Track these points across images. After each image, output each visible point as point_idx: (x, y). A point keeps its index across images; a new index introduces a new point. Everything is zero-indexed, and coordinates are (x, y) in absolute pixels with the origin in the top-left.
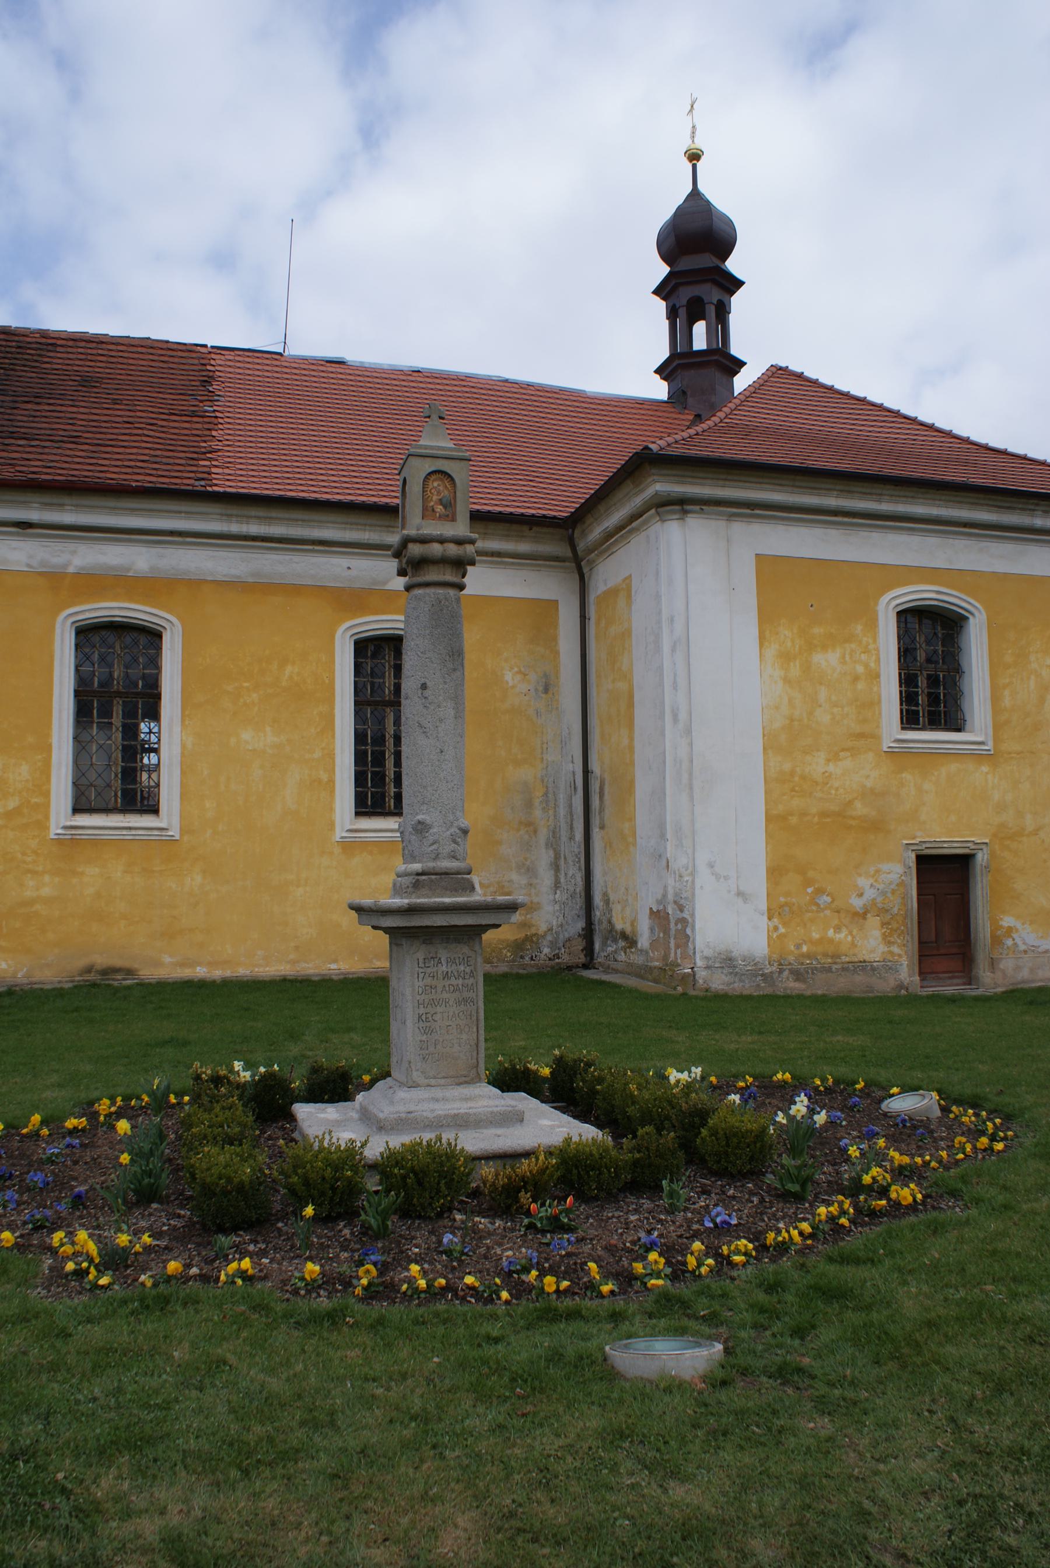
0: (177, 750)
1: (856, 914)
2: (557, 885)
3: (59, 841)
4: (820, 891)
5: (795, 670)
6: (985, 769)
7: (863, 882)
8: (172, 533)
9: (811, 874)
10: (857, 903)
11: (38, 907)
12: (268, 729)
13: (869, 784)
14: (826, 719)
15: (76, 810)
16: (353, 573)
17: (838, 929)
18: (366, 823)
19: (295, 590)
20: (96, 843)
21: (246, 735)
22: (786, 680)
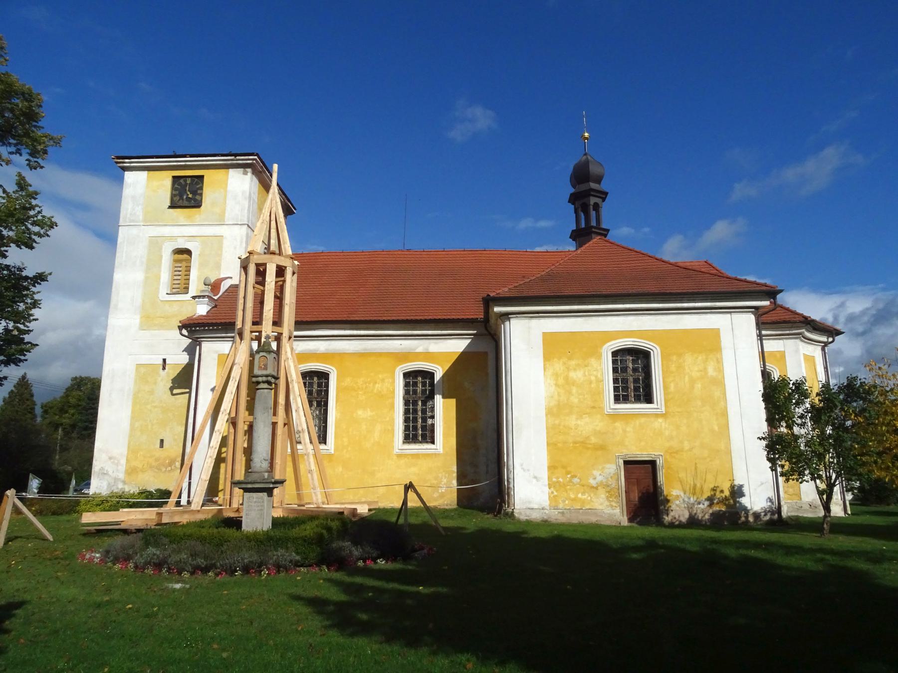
1: (592, 487)
2: (487, 472)
4: (575, 476)
5: (561, 381)
6: (660, 420)
7: (596, 473)
9: (569, 469)
10: (593, 482)
13: (598, 428)
14: (576, 401)
17: (583, 494)
18: (407, 446)
19: (380, 355)
21: (360, 412)
22: (556, 385)
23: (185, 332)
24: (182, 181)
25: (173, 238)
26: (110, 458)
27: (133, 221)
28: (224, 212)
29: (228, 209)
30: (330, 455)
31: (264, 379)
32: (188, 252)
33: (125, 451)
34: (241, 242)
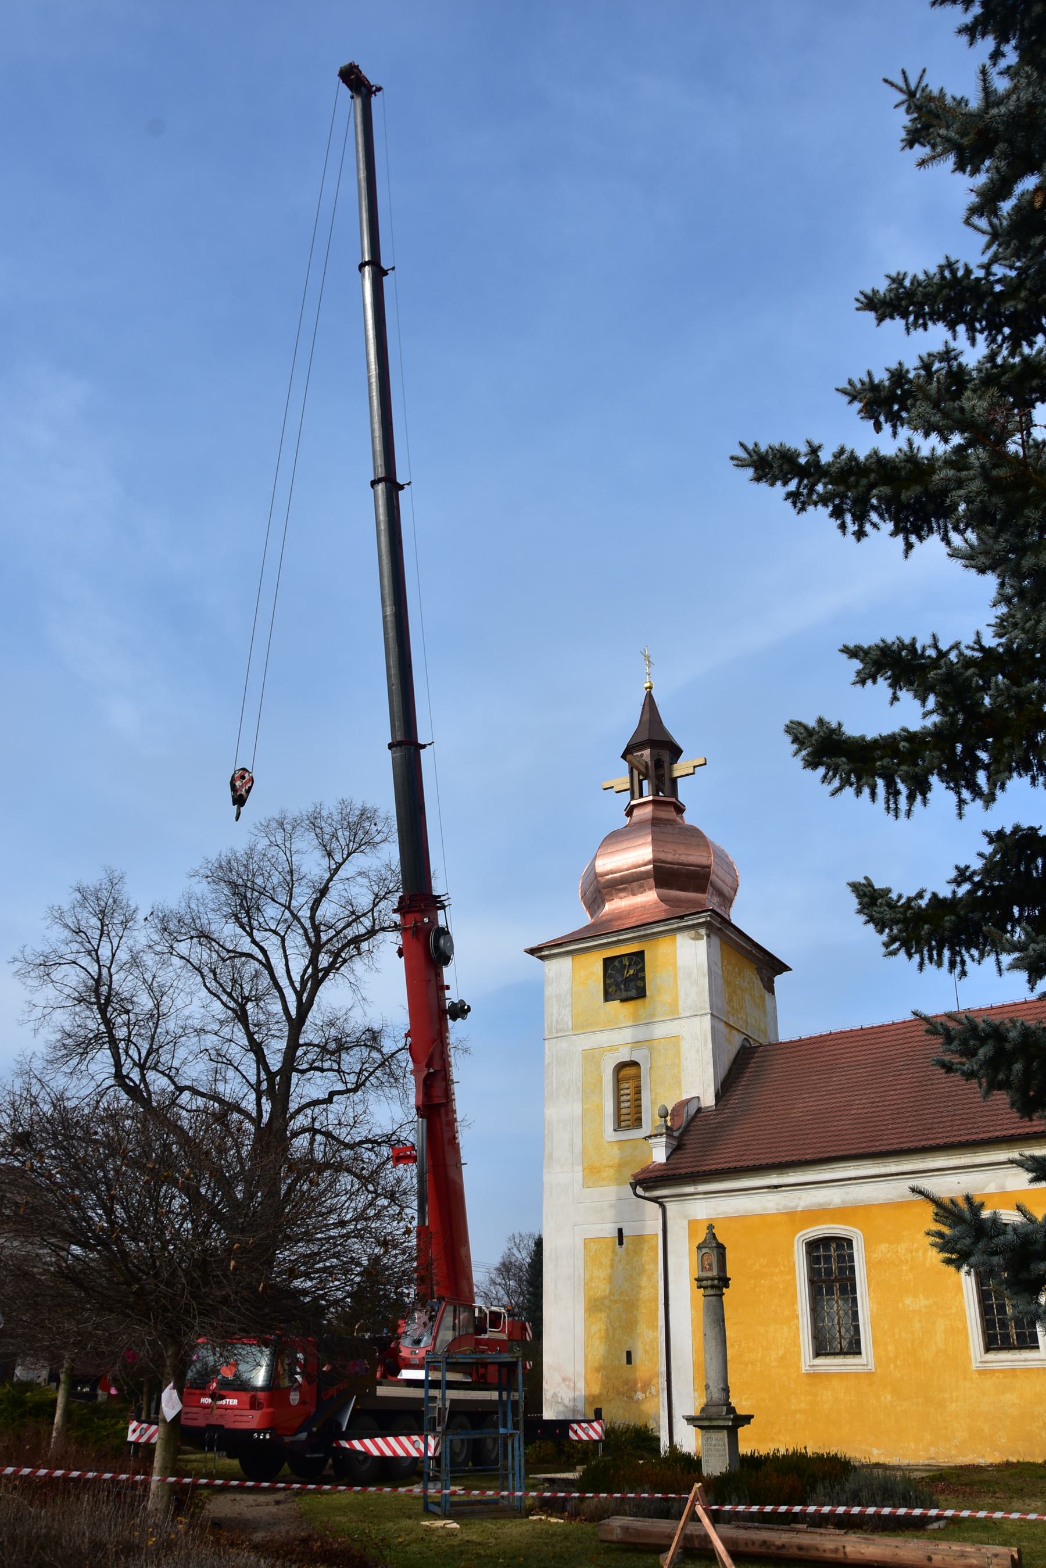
0: (867, 1314)
3: (808, 1375)
11: (798, 1416)
12: (921, 1296)
15: (817, 1354)
16: (962, 1185)
18: (991, 1356)
20: (828, 1375)
21: (908, 1301)
23: (640, 1191)
24: (616, 963)
25: (613, 1048)
26: (564, 1380)
27: (561, 1030)
28: (677, 1001)
29: (681, 994)
30: (869, 1374)
31: (709, 1283)
32: (634, 1064)
33: (580, 1368)
34: (706, 1041)
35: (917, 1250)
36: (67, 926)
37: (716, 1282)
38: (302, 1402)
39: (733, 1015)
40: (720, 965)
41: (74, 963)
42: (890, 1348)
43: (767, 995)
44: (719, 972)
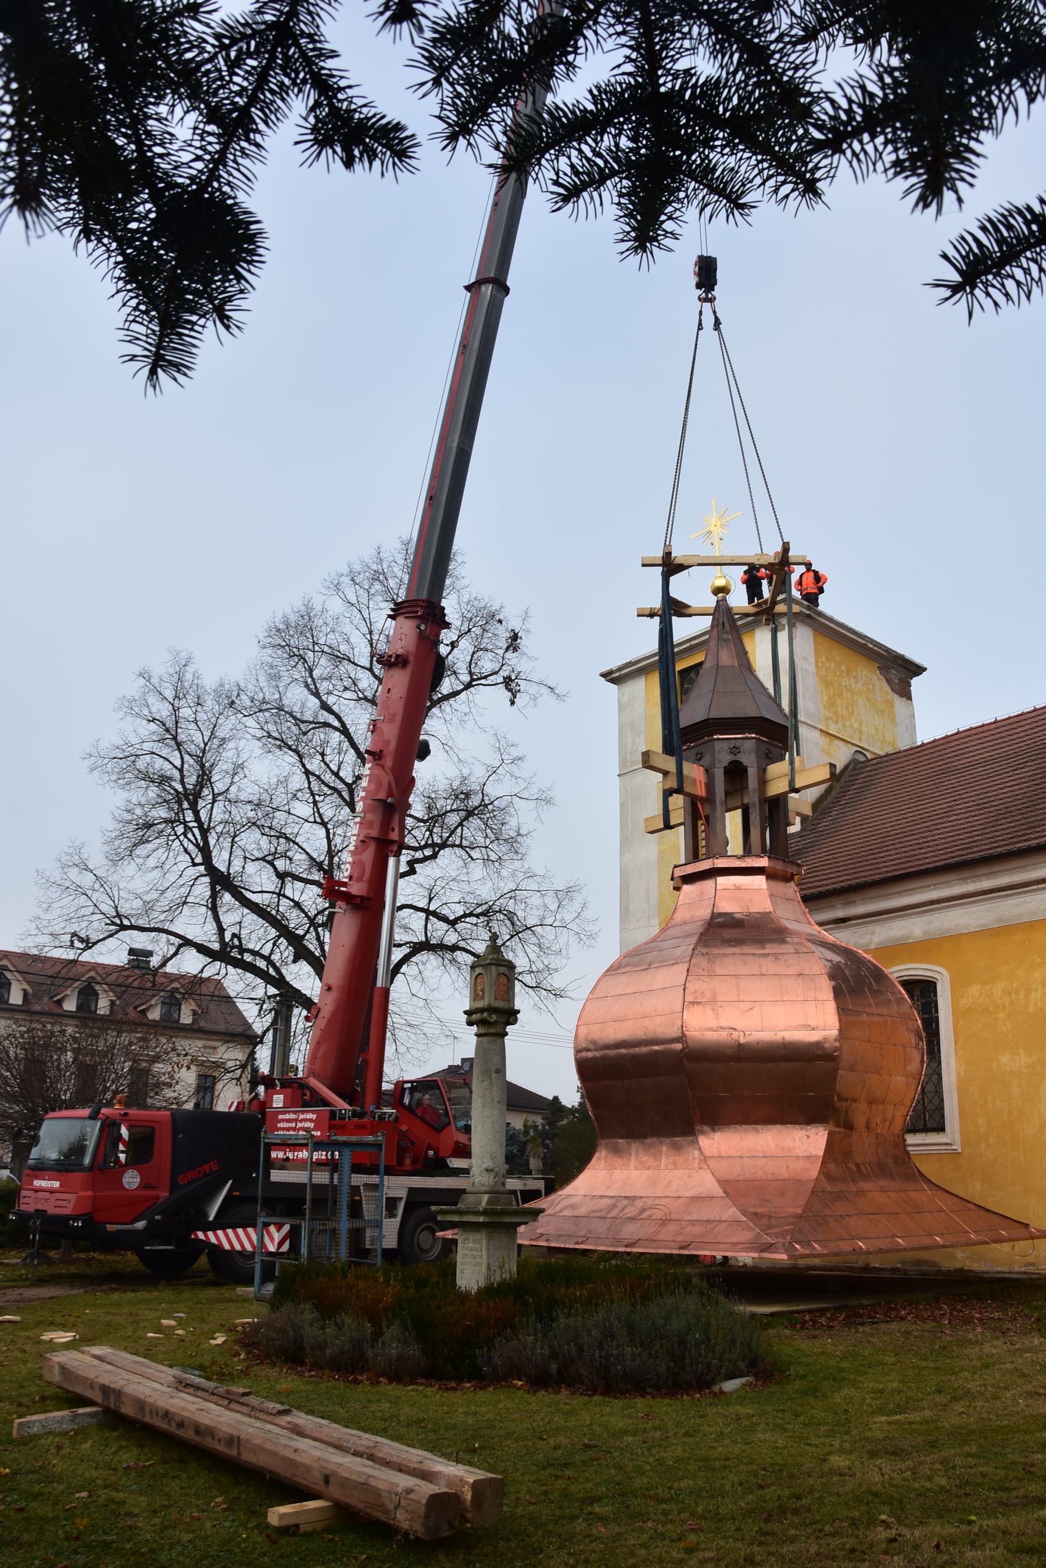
0: (954, 1077)
8: (932, 902)
12: (1022, 1051)
21: (1005, 1059)
30: (955, 1154)
35: (1017, 992)
36: (138, 715)
37: (485, 1014)
38: (144, 1185)
39: (837, 722)
40: (813, 660)
41: (153, 753)
42: (981, 1121)
43: (898, 701)
44: (812, 669)
